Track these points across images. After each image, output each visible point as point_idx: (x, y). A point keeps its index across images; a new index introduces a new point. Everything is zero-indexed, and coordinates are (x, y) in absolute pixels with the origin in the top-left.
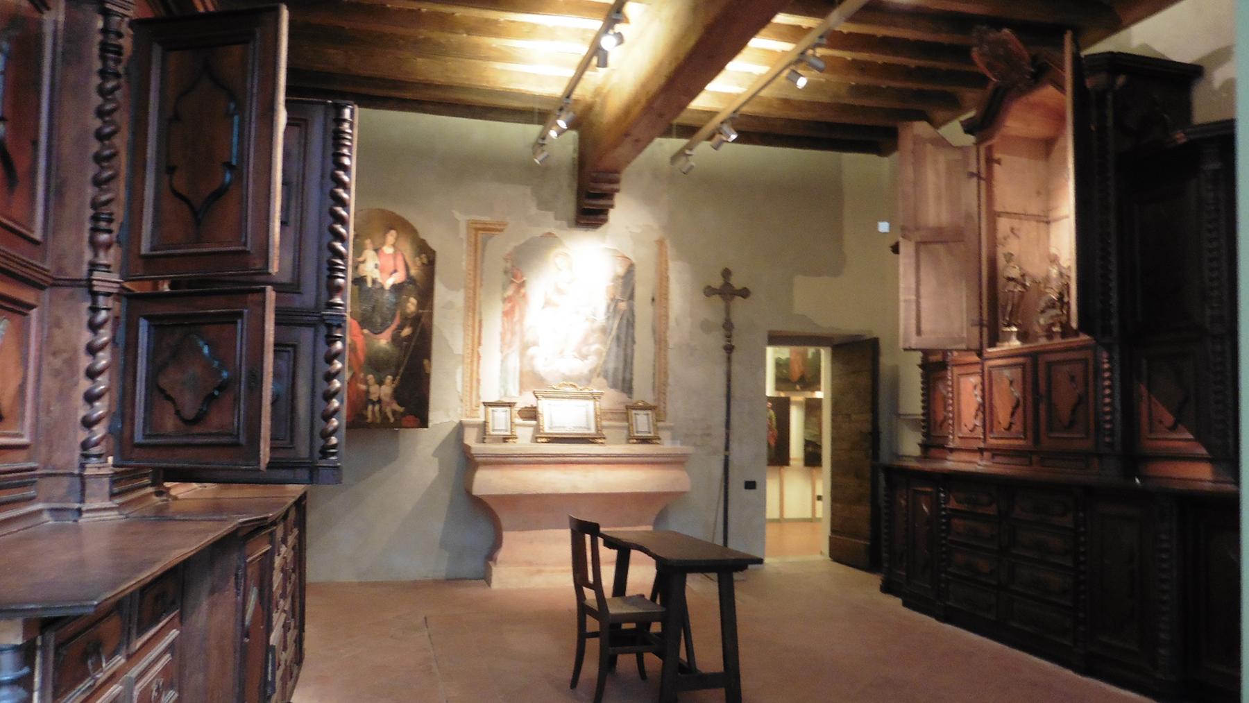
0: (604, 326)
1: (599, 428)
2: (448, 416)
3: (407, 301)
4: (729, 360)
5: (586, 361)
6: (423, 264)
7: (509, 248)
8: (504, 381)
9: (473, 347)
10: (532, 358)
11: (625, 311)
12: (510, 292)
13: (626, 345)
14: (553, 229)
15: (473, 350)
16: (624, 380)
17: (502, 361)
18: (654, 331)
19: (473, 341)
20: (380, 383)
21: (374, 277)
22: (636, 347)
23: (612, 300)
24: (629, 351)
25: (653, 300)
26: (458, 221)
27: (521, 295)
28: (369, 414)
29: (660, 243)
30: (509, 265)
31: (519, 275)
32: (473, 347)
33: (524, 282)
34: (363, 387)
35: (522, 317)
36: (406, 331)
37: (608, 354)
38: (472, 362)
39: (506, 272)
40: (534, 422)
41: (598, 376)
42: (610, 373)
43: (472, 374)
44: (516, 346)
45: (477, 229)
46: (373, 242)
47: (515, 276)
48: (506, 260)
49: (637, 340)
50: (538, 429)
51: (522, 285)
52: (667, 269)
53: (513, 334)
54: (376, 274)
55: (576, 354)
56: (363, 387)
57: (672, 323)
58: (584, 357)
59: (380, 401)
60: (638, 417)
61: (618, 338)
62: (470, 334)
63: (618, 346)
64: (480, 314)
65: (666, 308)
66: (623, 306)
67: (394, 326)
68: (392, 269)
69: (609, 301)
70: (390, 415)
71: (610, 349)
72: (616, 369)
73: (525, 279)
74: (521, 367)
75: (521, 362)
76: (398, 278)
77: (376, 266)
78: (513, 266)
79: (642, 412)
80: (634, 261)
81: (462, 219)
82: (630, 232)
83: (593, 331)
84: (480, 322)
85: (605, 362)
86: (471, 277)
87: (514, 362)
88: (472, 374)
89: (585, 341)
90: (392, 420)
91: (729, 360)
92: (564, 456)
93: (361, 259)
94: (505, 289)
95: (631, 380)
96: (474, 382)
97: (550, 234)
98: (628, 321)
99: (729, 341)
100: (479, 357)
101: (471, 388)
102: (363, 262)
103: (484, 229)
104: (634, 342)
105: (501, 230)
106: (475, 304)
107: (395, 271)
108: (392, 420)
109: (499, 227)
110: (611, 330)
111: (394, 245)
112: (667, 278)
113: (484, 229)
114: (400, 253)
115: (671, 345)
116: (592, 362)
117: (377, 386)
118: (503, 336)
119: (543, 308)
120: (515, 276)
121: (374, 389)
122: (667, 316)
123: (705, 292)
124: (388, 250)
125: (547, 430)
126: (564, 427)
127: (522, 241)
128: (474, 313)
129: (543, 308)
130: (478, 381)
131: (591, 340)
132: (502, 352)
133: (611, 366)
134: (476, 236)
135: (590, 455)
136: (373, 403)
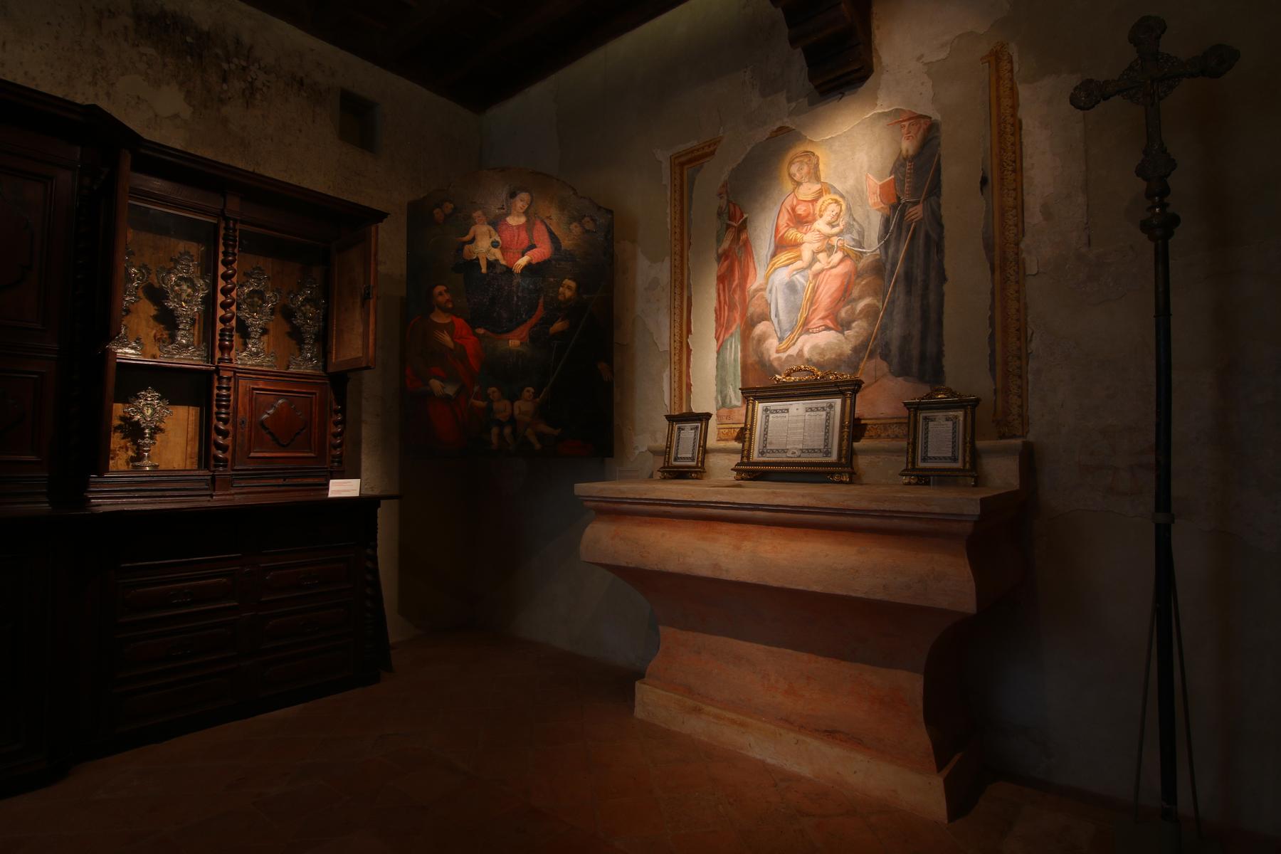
0: (878, 261)
1: (848, 456)
2: (656, 441)
3: (560, 284)
4: (1162, 258)
5: (846, 332)
6: (588, 231)
7: (724, 176)
8: (721, 382)
9: (681, 337)
10: (762, 339)
11: (919, 223)
12: (726, 245)
13: (926, 288)
14: (785, 120)
15: (681, 343)
16: (923, 357)
17: (718, 352)
18: (988, 247)
19: (681, 329)
20: (513, 398)
21: (492, 258)
22: (946, 287)
23: (893, 208)
24: (932, 297)
25: (984, 181)
26: (661, 162)
27: (741, 243)
28: (494, 439)
29: (996, 57)
30: (723, 202)
31: (738, 214)
32: (681, 337)
33: (745, 221)
34: (480, 404)
35: (744, 278)
36: (558, 326)
37: (889, 312)
38: (680, 360)
39: (720, 214)
40: (738, 445)
41: (871, 356)
42: (894, 347)
43: (680, 377)
44: (736, 328)
45: (682, 165)
46: (485, 214)
47: (732, 217)
48: (720, 195)
49: (949, 274)
50: (745, 453)
51: (743, 227)
52: (1015, 107)
53: (732, 308)
54: (497, 254)
55: (828, 322)
56: (480, 404)
57: (1034, 217)
58: (842, 326)
59: (512, 420)
60: (931, 424)
61: (908, 277)
62: (678, 320)
63: (909, 292)
64: (689, 286)
65: (1019, 190)
66: (917, 212)
67: (533, 321)
68: (526, 243)
69: (887, 211)
70: (533, 439)
71: (892, 302)
72: (906, 339)
73: (745, 216)
74: (744, 357)
75: (744, 350)
76: (542, 251)
77: (495, 245)
78: (729, 202)
79: (940, 415)
80: (936, 117)
81: (663, 157)
82: (925, 64)
83: (858, 274)
84: (689, 299)
85: (884, 328)
86: (678, 236)
87: (734, 351)
88: (680, 377)
89: (845, 295)
90: (538, 446)
91: (1162, 258)
92: (698, 504)
93: (467, 238)
94: (719, 241)
95: (940, 354)
96: (684, 387)
97: (781, 129)
98: (927, 236)
99: (1164, 206)
100: (689, 351)
101: (681, 399)
102: (473, 240)
103: (690, 161)
104: (943, 279)
105: (713, 153)
106: (682, 274)
107: (532, 247)
108: (538, 446)
109: (707, 150)
110: (894, 265)
111: (526, 213)
112: (1018, 126)
113: (690, 161)
114: (538, 222)
115: (1032, 268)
116: (859, 328)
117: (507, 402)
118: (718, 312)
119: (774, 255)
120: (732, 217)
121: (502, 407)
122: (1020, 207)
123: (1074, 101)
124: (515, 220)
125: (755, 457)
126: (785, 451)
127: (740, 160)
128: (682, 289)
129: (774, 255)
130: (689, 386)
131: (856, 292)
132: (717, 339)
133: (896, 332)
134: (682, 174)
135: (742, 507)
136: (501, 425)
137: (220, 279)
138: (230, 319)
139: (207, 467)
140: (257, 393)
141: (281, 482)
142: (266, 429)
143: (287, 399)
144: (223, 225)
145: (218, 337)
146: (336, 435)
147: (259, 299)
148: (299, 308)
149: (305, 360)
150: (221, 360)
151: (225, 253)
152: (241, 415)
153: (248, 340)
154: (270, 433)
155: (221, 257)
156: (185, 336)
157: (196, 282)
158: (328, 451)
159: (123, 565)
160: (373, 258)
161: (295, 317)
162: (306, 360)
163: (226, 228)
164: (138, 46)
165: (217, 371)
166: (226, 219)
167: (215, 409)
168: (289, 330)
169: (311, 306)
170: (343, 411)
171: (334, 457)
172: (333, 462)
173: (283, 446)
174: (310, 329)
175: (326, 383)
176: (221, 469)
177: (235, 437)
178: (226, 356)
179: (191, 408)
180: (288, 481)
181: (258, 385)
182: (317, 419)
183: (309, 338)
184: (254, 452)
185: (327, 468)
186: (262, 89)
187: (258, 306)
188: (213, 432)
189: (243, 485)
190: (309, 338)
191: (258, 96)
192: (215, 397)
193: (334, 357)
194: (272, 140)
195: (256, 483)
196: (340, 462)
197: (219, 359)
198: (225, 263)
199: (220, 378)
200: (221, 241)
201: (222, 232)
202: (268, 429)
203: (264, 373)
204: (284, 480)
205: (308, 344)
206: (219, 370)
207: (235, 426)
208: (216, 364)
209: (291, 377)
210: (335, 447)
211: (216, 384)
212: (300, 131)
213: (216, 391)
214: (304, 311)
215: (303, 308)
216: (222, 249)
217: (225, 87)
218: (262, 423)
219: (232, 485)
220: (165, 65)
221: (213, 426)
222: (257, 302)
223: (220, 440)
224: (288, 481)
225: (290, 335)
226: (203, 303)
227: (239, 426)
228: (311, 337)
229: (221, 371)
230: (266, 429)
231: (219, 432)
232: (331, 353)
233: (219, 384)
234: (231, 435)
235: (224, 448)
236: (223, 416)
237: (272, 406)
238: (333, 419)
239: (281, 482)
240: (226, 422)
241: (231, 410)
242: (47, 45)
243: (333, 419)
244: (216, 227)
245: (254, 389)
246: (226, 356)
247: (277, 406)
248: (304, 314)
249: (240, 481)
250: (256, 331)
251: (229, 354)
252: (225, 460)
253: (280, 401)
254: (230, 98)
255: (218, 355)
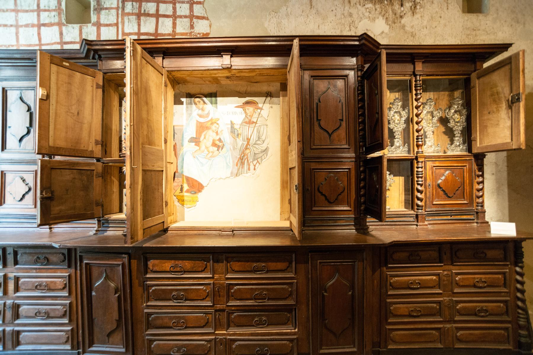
137: (414, 109)
138: (420, 130)
139: (413, 208)
140: (435, 169)
141: (449, 217)
142: (440, 188)
143: (451, 170)
144: (414, 80)
145: (415, 140)
146: (478, 190)
147: (430, 116)
148: (452, 117)
149: (456, 146)
150: (418, 152)
151: (416, 95)
152: (428, 182)
153: (426, 139)
154: (443, 191)
155: (414, 97)
156: (398, 141)
157: (401, 113)
158: (474, 200)
159: (390, 266)
160: (521, 73)
161: (449, 122)
162: (457, 147)
163: (416, 81)
164: (365, 5)
165: (417, 158)
166: (415, 75)
167: (416, 179)
168: (444, 130)
169: (458, 115)
170: (482, 176)
171: (477, 203)
172: (477, 206)
173: (450, 197)
174: (458, 129)
175: (472, 159)
176: (420, 211)
177: (426, 194)
178: (420, 150)
179: (400, 177)
180: (453, 217)
181: (435, 164)
182: (468, 181)
183: (458, 133)
184: (436, 201)
185: (474, 210)
186: (420, 3)
187: (430, 120)
188: (416, 191)
189: (430, 219)
190: (458, 133)
191: (418, 7)
192: (415, 173)
193: (478, 143)
194: (426, 28)
195: (436, 218)
196: (482, 206)
197: (417, 152)
198: (417, 100)
199: (418, 162)
200: (414, 88)
201: (414, 83)
202: (442, 188)
203: (439, 157)
204: (451, 217)
205: (457, 137)
206: (418, 158)
207: (425, 187)
208: (415, 155)
209: (444, 158)
210: (478, 197)
211: (416, 165)
212: (441, 17)
213: (416, 169)
214: (454, 118)
215: (453, 117)
216: (414, 92)
217: (402, 9)
218: (439, 186)
219: (425, 219)
220: (376, 10)
221: (416, 188)
222: (457, 117)
223: (419, 195)
224: (453, 217)
225: (445, 133)
226: (405, 123)
227: (427, 187)
228: (459, 133)
229: (419, 158)
230: (440, 188)
231: (418, 191)
232: (476, 141)
233: (417, 165)
234: (424, 192)
235: (421, 200)
236: (420, 182)
237: (443, 175)
238: (476, 181)
239: (449, 217)
240: (421, 185)
241: (423, 179)
242: (332, 20)
243: (476, 181)
244: (410, 81)
245: (434, 166)
246: (420, 150)
247: (446, 175)
248: (454, 120)
249: (429, 217)
250: (430, 134)
251: (421, 149)
252: (422, 207)
253: (447, 172)
254: (405, 14)
255: (416, 150)
